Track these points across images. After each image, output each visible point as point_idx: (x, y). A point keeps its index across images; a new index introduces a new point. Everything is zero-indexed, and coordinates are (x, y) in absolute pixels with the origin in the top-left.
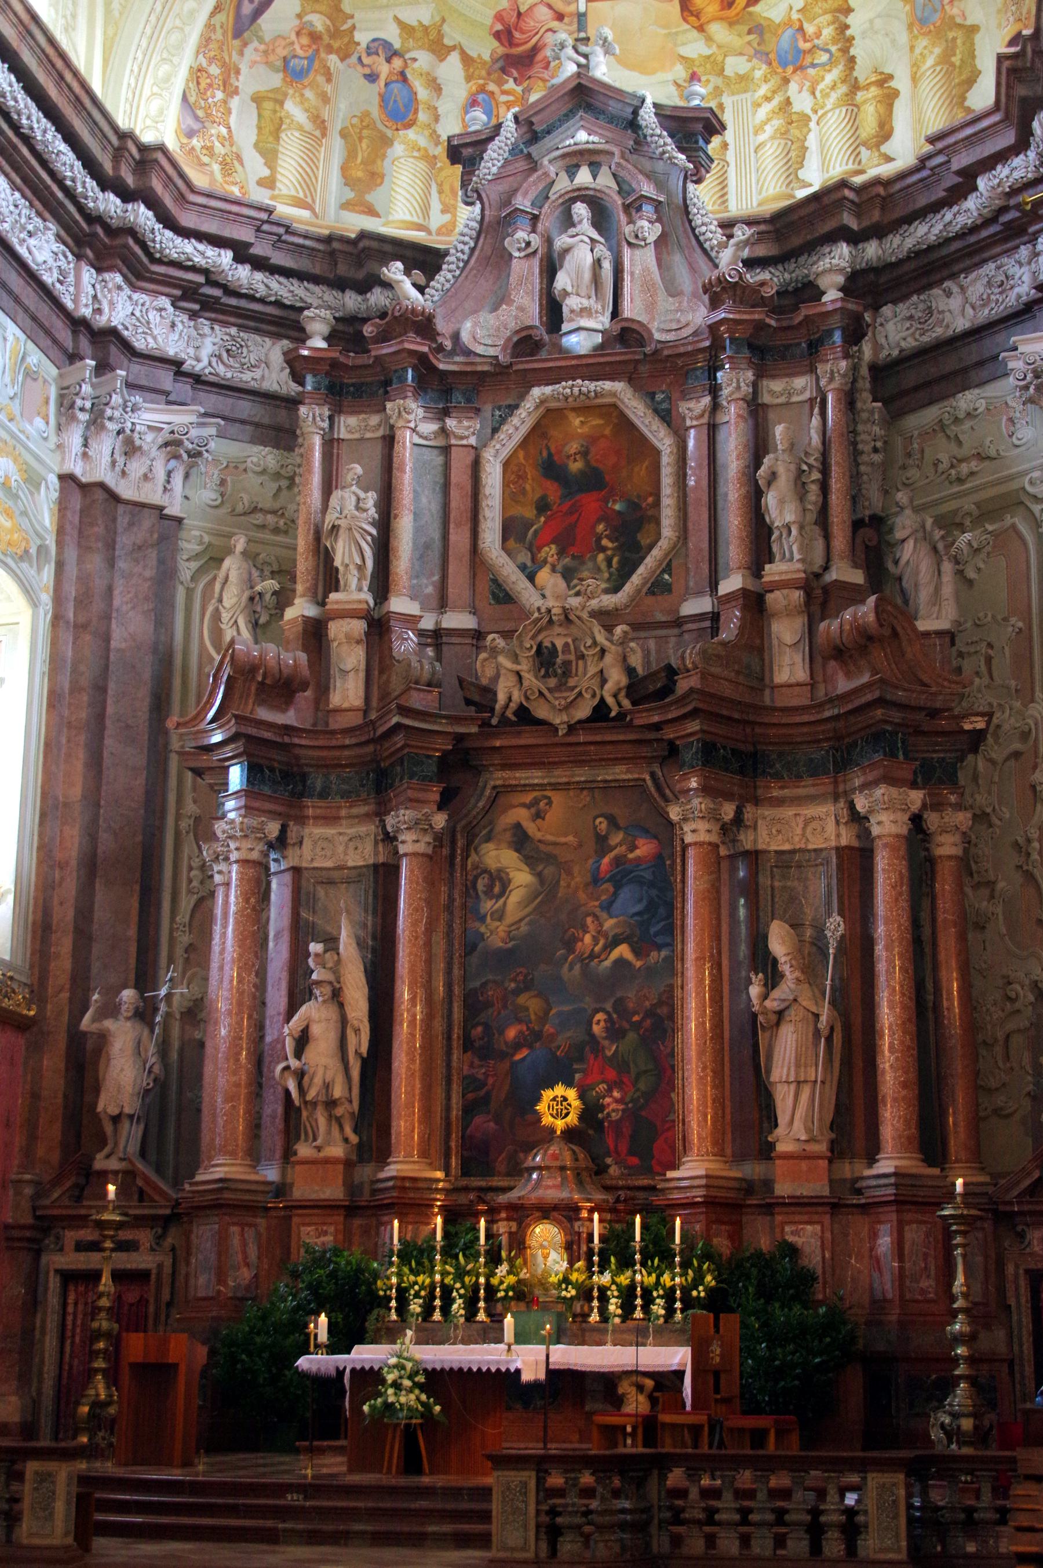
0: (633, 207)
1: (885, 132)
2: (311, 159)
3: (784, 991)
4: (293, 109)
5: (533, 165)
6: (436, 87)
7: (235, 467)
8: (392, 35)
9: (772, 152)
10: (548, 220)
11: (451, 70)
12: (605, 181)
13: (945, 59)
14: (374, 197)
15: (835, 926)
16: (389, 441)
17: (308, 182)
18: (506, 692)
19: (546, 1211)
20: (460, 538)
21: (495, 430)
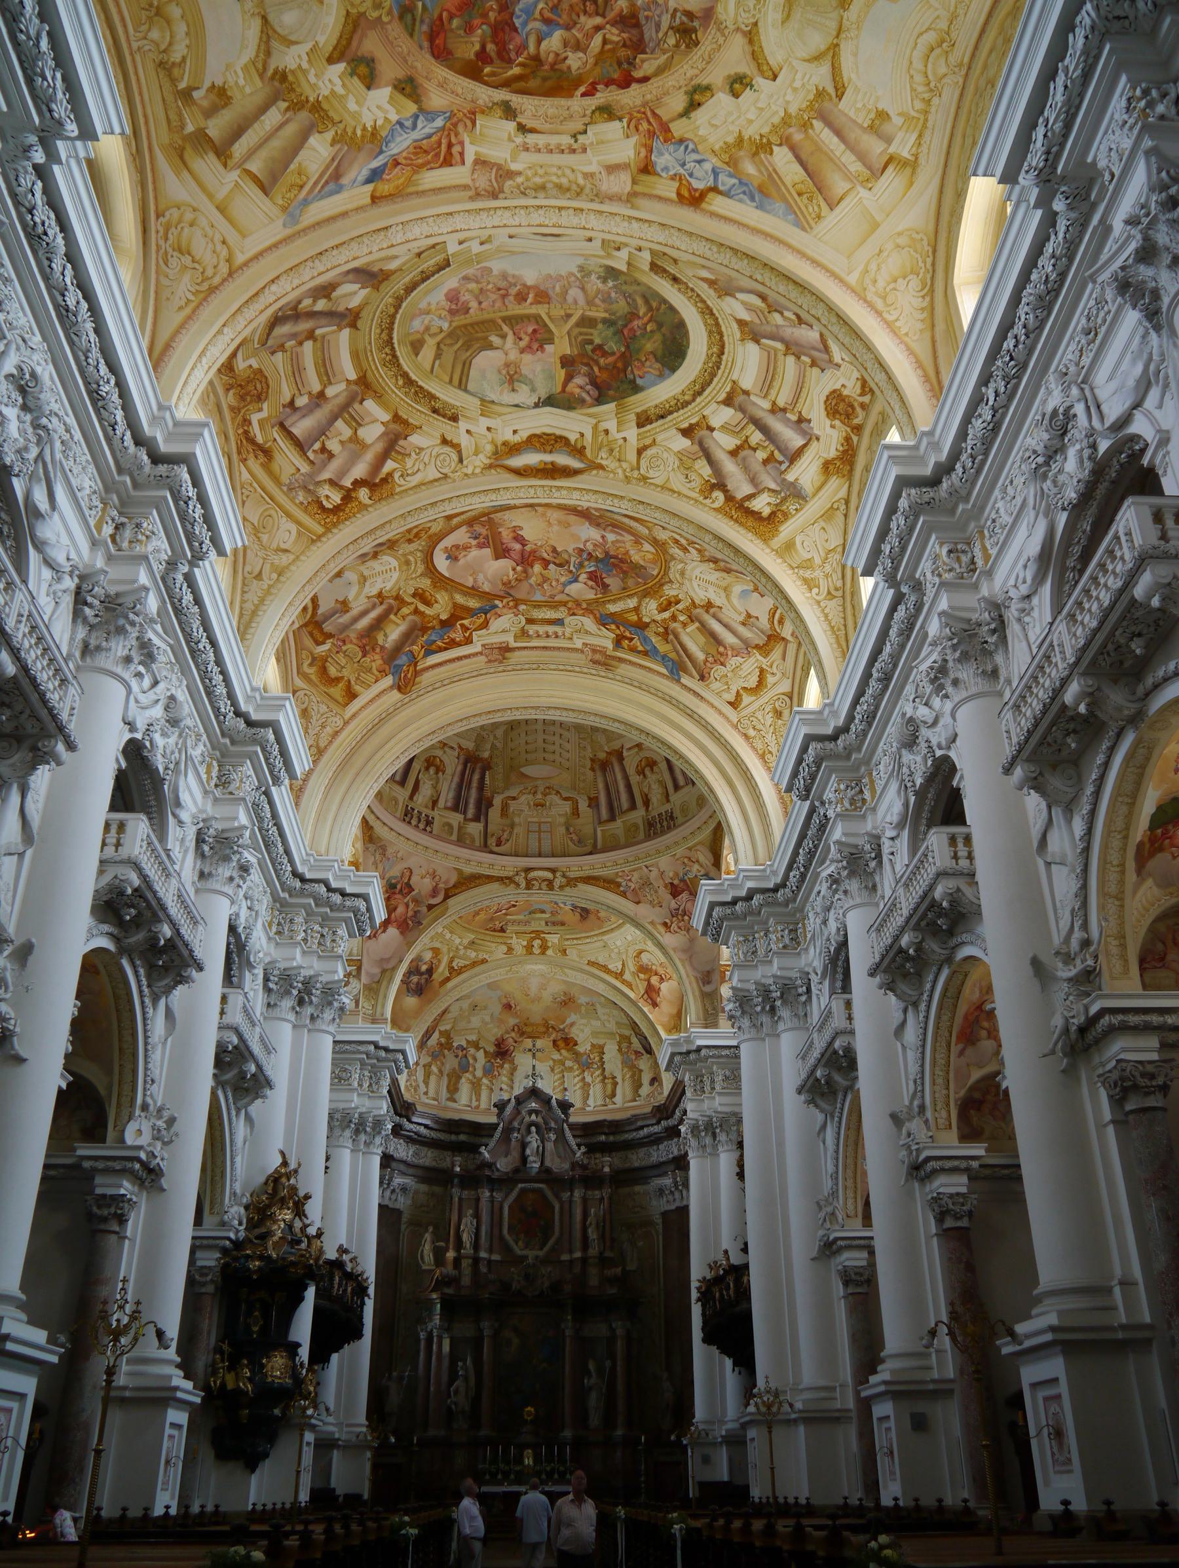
0: (549, 1129)
1: (613, 1095)
2: (438, 1084)
3: (593, 1380)
4: (434, 1069)
5: (519, 1113)
6: (475, 1059)
7: (416, 1192)
8: (464, 1044)
9: (579, 1092)
10: (523, 1131)
11: (480, 1055)
12: (540, 1120)
13: (632, 1076)
14: (456, 1096)
15: (608, 1363)
16: (478, 1200)
17: (437, 1092)
18: (515, 1286)
19: (527, 1446)
20: (496, 1231)
21: (507, 1196)
